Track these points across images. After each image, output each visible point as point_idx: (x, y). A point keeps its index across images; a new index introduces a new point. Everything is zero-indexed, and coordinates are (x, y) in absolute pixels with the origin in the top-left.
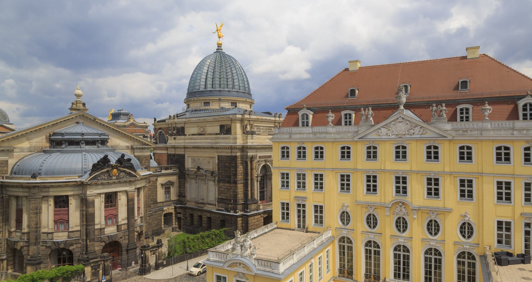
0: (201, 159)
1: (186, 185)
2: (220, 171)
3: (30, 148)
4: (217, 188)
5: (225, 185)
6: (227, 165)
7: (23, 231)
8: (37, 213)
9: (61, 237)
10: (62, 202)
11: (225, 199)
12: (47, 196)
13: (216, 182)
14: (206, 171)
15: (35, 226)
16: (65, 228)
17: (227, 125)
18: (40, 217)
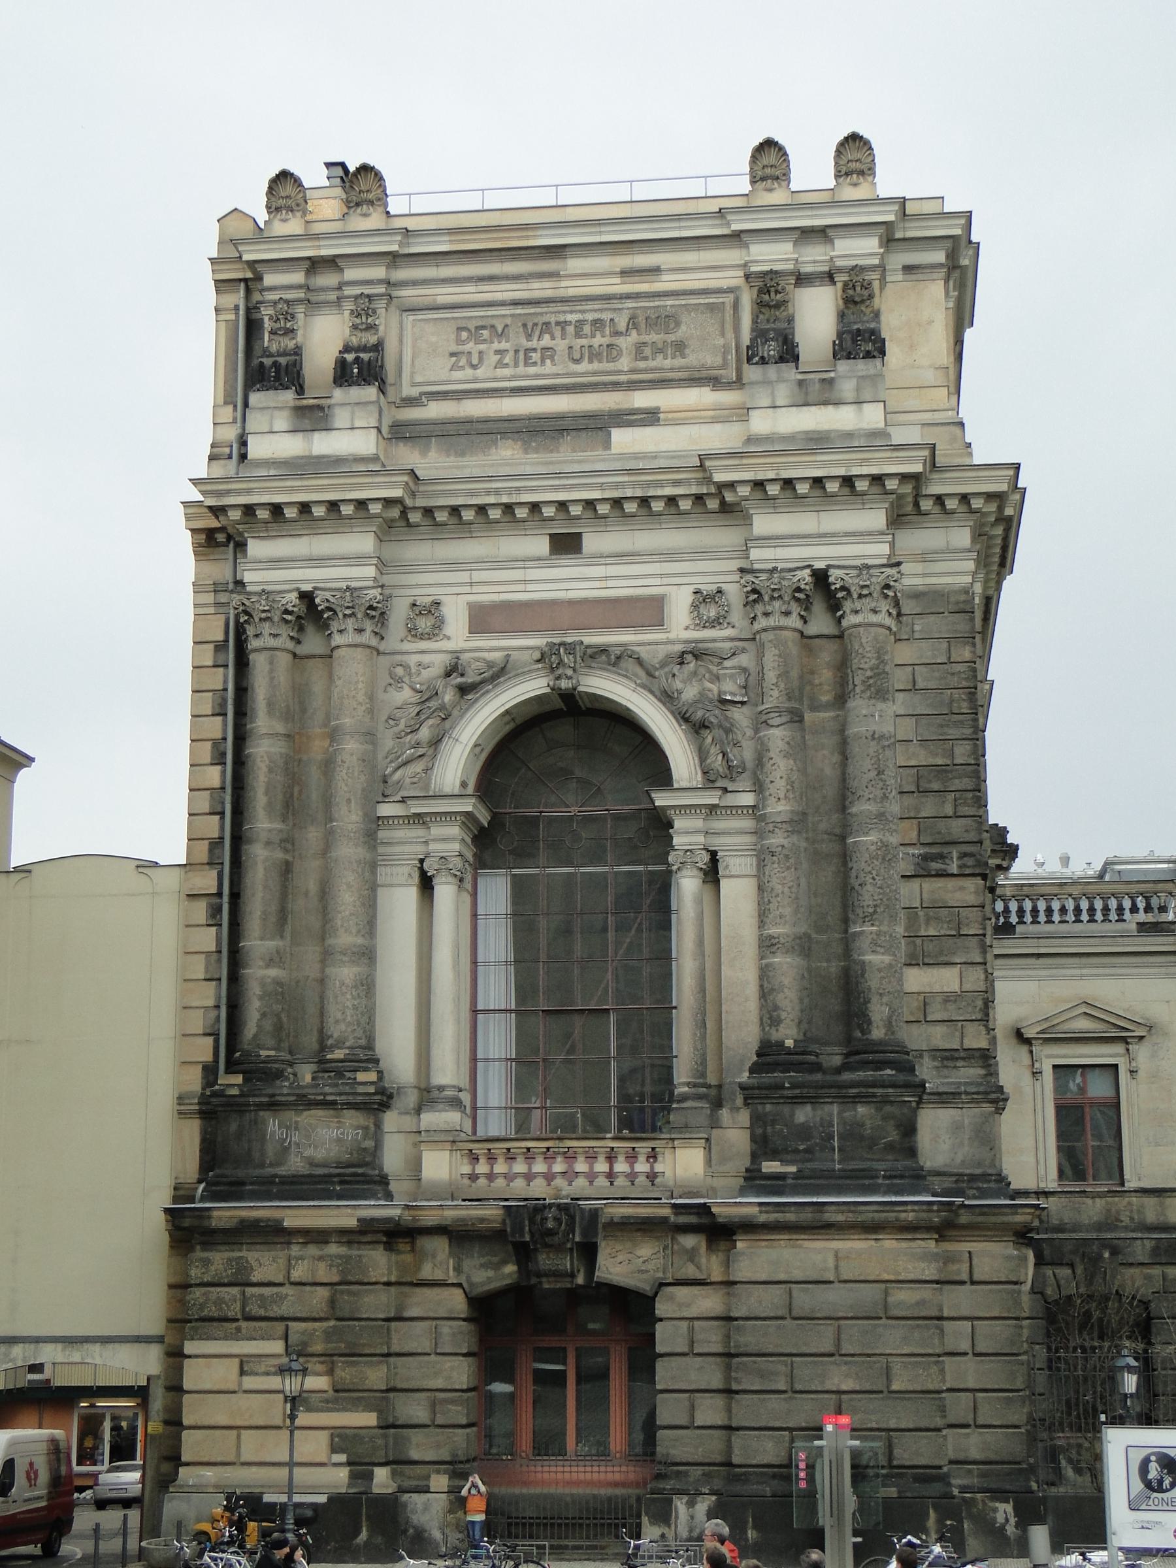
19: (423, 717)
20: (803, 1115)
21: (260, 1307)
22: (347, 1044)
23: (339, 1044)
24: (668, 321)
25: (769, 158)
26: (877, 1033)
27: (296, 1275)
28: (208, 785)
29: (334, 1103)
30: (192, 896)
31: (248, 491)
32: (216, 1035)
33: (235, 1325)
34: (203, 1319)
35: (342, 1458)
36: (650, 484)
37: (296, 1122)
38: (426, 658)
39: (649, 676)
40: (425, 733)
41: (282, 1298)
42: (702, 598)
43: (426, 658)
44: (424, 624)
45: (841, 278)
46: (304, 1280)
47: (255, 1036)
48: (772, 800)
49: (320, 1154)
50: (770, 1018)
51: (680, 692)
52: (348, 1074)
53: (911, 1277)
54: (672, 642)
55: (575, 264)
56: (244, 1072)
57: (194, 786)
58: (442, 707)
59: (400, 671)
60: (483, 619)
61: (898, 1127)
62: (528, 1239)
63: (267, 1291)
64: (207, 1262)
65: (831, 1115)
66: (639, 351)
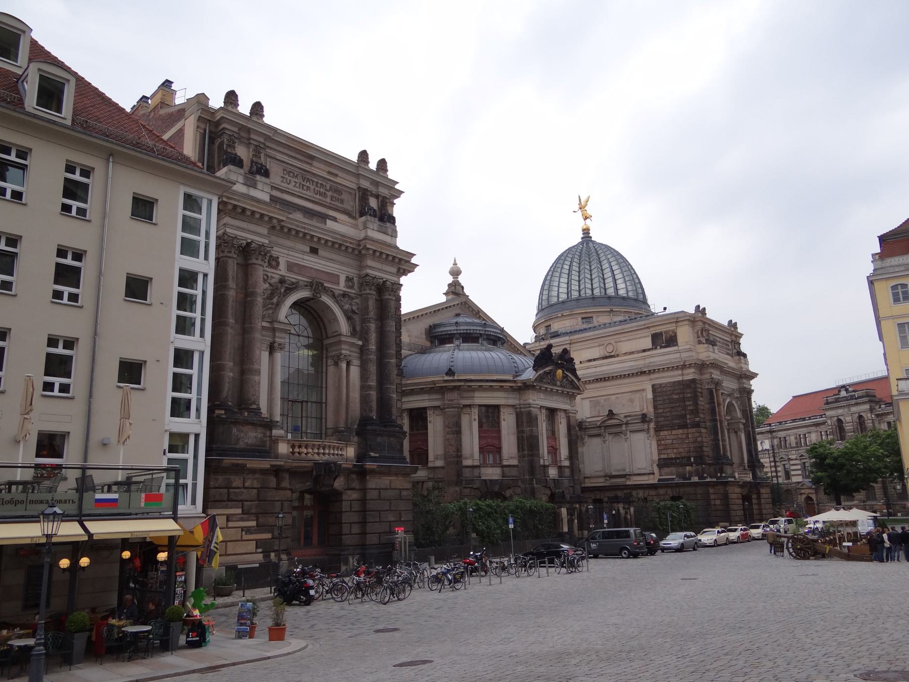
0: (613, 397)
1: (580, 450)
2: (660, 411)
3: (410, 344)
4: (654, 443)
5: (674, 432)
6: (675, 397)
7: (430, 465)
9: (492, 473)
10: (490, 416)
11: (676, 458)
12: (470, 406)
13: (652, 431)
14: (626, 417)
15: (455, 454)
16: (495, 460)
17: (666, 332)
18: (460, 440)
20: (379, 439)
24: (339, 192)
25: (364, 155)
26: (394, 417)
27: (247, 484)
31: (238, 201)
35: (260, 550)
40: (275, 300)
42: (349, 279)
43: (274, 275)
44: (274, 263)
45: (380, 198)
49: (250, 441)
55: (315, 163)
60: (291, 267)
63: (236, 490)
64: (217, 479)
66: (332, 197)
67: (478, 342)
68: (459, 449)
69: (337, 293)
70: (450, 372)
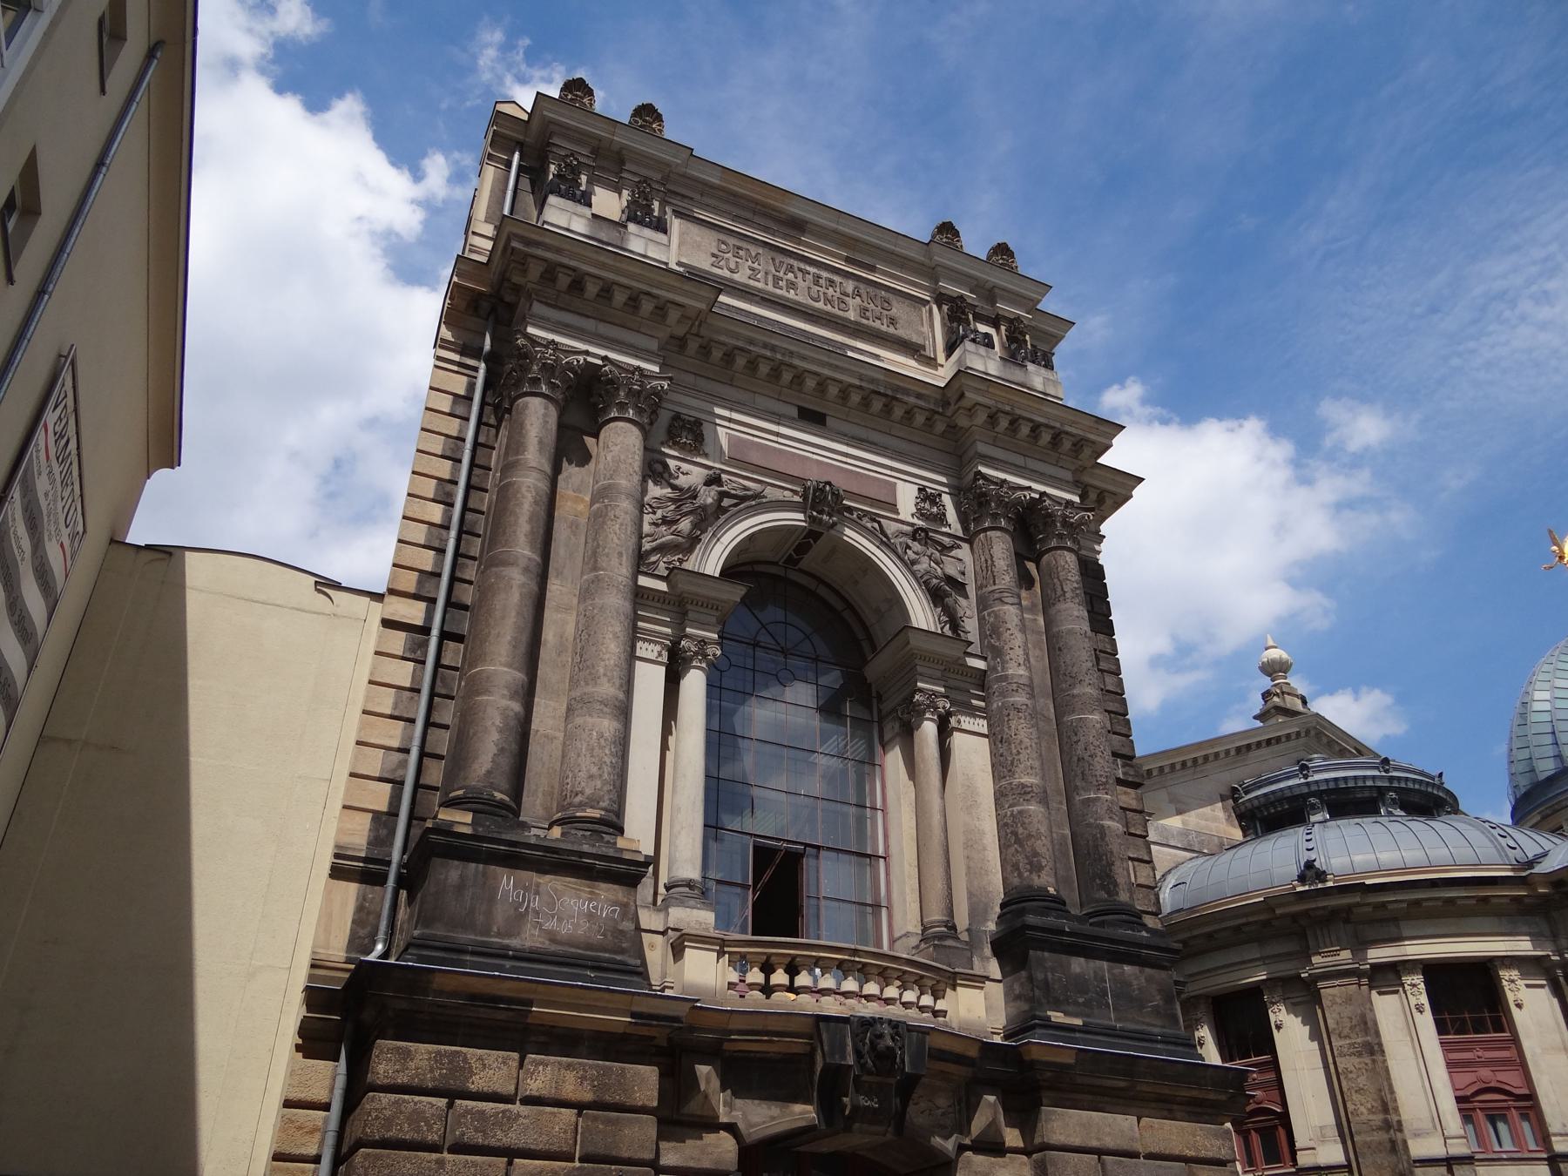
8: (1372, 1053)
15: (1377, 1119)
16: (1516, 1137)
19: (685, 509)
20: (1078, 965)
21: (476, 1130)
22: (602, 804)
23: (592, 802)
28: (426, 518)
29: (590, 868)
30: (387, 623)
31: (558, 251)
32: (398, 784)
33: (434, 1156)
34: (385, 1144)
36: (898, 389)
37: (538, 885)
38: (685, 467)
39: (885, 543)
41: (513, 1118)
42: (926, 497)
46: (544, 1093)
47: (489, 772)
48: (1012, 664)
49: (565, 929)
50: (1031, 863)
51: (913, 562)
52: (607, 837)
53: (1210, 1154)
54: (903, 522)
56: (474, 811)
57: (410, 514)
58: (704, 508)
59: (659, 468)
61: (1160, 991)
62: (850, 1061)
63: (488, 1106)
64: (407, 1055)
65: (1101, 969)
67: (1377, 812)
68: (1386, 1104)
69: (891, 528)
70: (1310, 871)
